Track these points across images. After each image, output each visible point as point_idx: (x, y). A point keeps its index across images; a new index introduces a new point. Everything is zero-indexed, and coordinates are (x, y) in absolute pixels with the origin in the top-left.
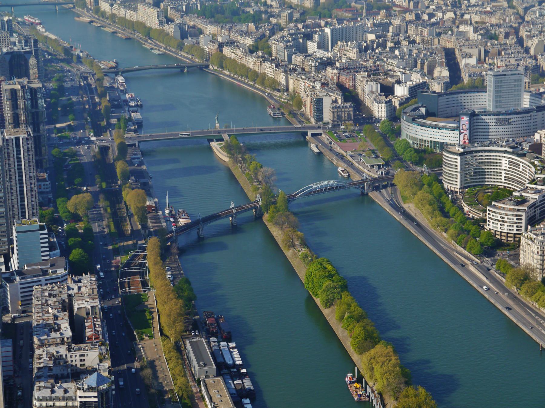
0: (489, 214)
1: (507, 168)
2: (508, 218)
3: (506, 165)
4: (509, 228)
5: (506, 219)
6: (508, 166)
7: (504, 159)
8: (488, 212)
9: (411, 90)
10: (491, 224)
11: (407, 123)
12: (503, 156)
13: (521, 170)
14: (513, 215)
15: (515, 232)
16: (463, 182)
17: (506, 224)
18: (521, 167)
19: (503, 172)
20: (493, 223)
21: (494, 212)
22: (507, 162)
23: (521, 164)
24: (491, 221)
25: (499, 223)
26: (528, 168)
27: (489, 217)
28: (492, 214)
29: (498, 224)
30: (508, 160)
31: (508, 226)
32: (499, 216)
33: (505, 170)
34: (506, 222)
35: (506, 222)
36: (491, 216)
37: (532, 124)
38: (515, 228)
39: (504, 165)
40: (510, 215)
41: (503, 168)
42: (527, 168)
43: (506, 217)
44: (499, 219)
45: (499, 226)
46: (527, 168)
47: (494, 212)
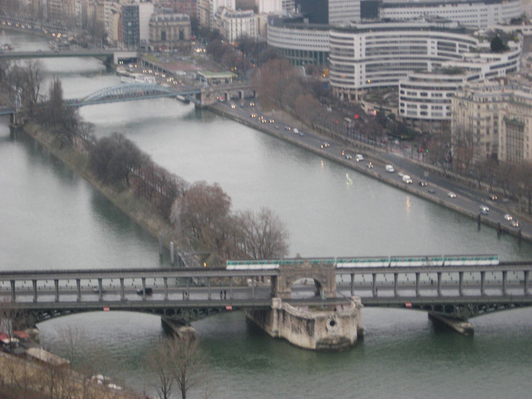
0: (402, 92)
1: (436, 56)
2: (432, 95)
3: (433, 51)
4: (435, 111)
5: (429, 97)
6: (436, 51)
7: (429, 40)
8: (400, 89)
9: (287, 6)
10: (405, 108)
11: (275, 29)
12: (427, 36)
13: (457, 53)
14: (442, 89)
15: (444, 117)
16: (364, 80)
17: (429, 105)
18: (458, 48)
19: (429, 63)
20: (409, 106)
21: (409, 87)
22: (435, 45)
23: (457, 43)
24: (406, 103)
25: (419, 104)
26: (468, 45)
27: (402, 98)
28: (406, 90)
29: (416, 107)
30: (436, 41)
31: (433, 108)
32: (419, 92)
33: (432, 59)
34: (429, 101)
35: (429, 101)
36: (405, 95)
37: (479, 13)
38: (445, 111)
39: (429, 50)
40: (437, 89)
41: (429, 55)
42: (465, 47)
43: (429, 93)
44: (419, 96)
45: (419, 110)
46: (465, 47)
47: (409, 87)
